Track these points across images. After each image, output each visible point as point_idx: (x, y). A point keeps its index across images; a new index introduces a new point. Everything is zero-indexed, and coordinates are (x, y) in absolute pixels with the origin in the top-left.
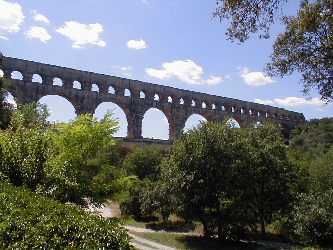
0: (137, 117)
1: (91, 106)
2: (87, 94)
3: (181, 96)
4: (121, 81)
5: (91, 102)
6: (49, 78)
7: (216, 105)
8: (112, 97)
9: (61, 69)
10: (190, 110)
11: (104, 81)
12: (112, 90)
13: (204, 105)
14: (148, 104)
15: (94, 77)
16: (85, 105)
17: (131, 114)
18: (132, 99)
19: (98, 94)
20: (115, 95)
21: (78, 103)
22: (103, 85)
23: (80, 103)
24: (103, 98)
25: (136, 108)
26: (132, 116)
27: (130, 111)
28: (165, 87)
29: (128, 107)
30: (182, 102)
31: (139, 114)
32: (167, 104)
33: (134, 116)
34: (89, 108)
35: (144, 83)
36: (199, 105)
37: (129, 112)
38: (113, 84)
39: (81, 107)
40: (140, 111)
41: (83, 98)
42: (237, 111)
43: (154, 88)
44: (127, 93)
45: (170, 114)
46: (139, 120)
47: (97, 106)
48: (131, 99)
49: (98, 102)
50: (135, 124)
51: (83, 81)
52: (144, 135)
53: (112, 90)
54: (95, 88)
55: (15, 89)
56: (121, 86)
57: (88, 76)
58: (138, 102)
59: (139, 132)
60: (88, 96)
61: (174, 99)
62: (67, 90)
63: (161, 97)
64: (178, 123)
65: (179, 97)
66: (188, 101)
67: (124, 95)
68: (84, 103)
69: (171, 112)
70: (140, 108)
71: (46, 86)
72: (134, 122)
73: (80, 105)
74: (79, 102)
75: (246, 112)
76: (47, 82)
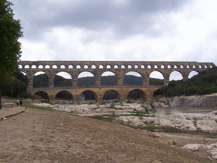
4: (89, 62)
6: (59, 66)
13: (136, 67)
31: (99, 76)
36: (133, 67)
41: (73, 72)
42: (159, 67)
49: (80, 73)
54: (78, 67)
55: (47, 72)
56: (90, 65)
65: (120, 65)
66: (126, 66)
70: (99, 73)
74: (71, 74)
76: (59, 68)
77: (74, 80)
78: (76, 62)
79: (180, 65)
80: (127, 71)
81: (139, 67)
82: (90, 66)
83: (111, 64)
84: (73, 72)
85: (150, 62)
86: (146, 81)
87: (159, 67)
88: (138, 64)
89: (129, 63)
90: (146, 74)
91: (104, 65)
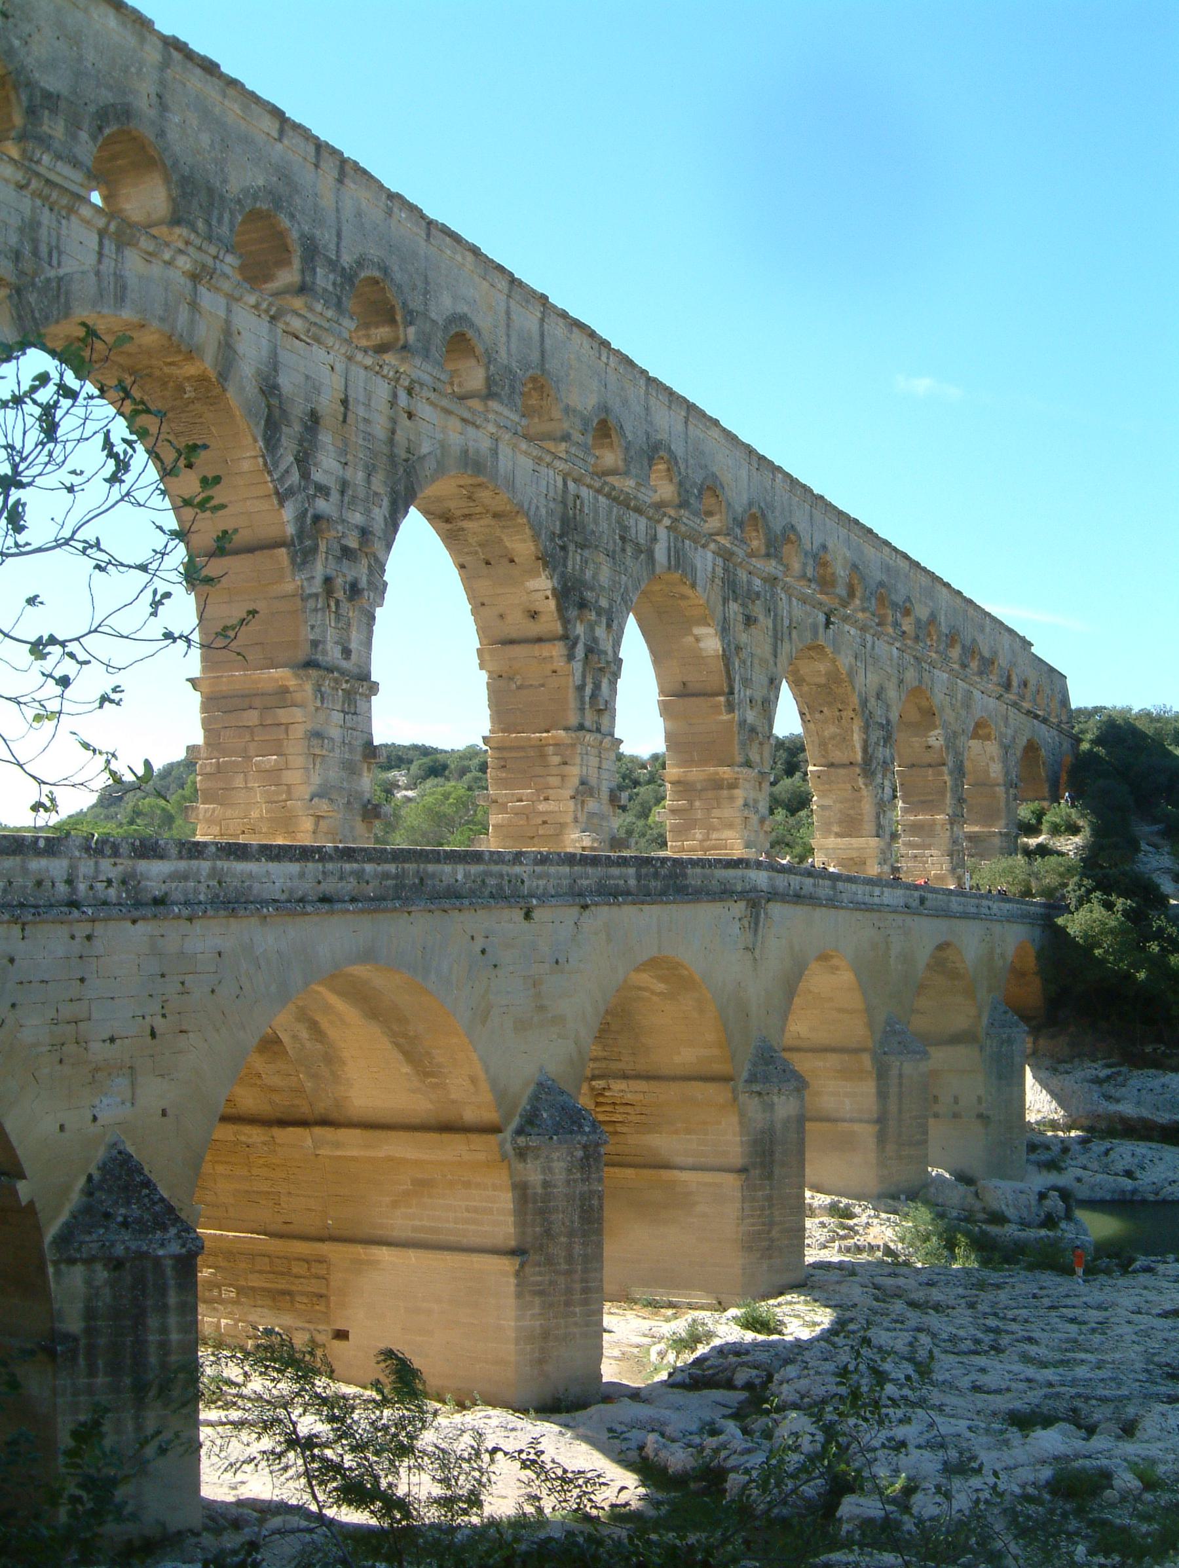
1: (357, 518)
5: (360, 475)
10: (786, 623)
17: (566, 622)
18: (571, 485)
21: (283, 467)
23: (295, 477)
24: (425, 449)
28: (691, 409)
33: (580, 651)
34: (353, 543)
39: (301, 517)
41: (314, 418)
68: (317, 476)
69: (724, 631)
71: (46, 217)
77: (333, 654)
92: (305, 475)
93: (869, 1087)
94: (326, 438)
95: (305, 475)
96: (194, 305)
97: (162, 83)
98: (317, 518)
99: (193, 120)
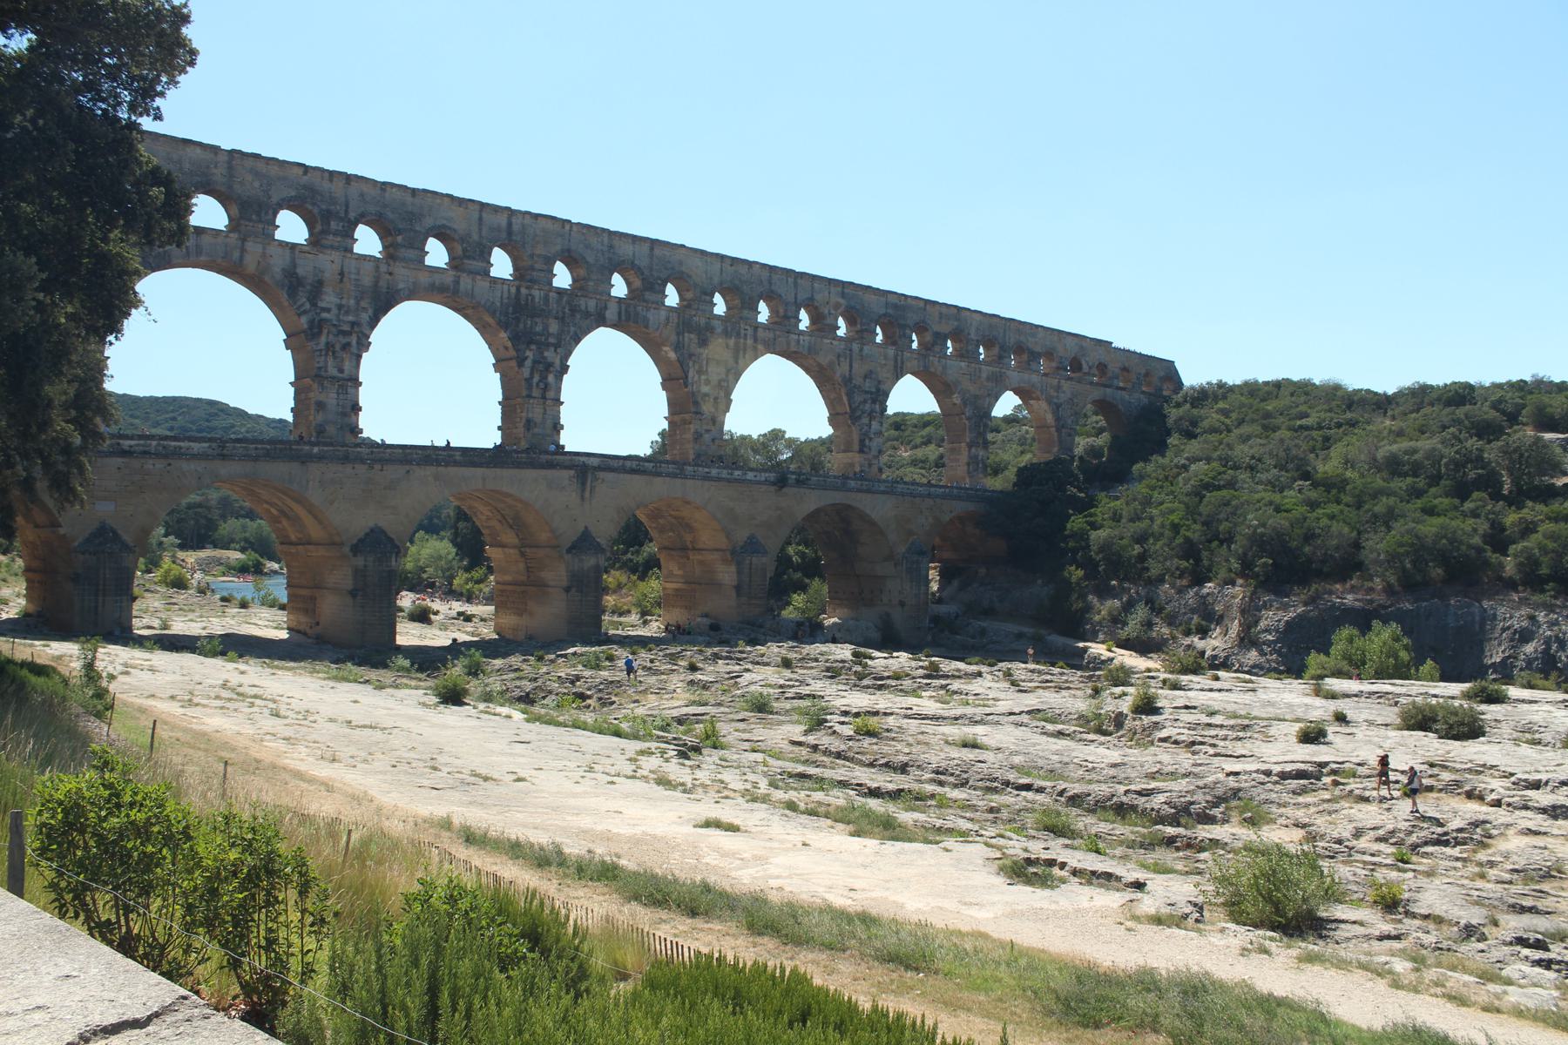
0: (541, 367)
1: (351, 318)
2: (336, 267)
3: (716, 280)
5: (352, 302)
7: (850, 322)
8: (437, 279)
9: (223, 158)
11: (405, 213)
12: (436, 254)
13: (805, 321)
14: (587, 314)
15: (362, 195)
16: (325, 315)
18: (524, 291)
19: (383, 268)
20: (452, 273)
22: (400, 232)
23: (308, 306)
24: (401, 286)
25: (539, 328)
26: (521, 363)
27: (515, 338)
28: (654, 243)
29: (505, 326)
30: (720, 307)
31: (549, 354)
32: (663, 313)
33: (528, 363)
34: (346, 328)
35: (567, 227)
36: (783, 320)
37: (509, 344)
38: (444, 226)
39: (311, 322)
40: (551, 340)
43: (611, 247)
44: (501, 265)
45: (672, 355)
46: (551, 378)
47: (378, 320)
48: (518, 289)
49: (384, 303)
50: (536, 393)
51: (316, 211)
52: (574, 439)
53: (436, 254)
54: (367, 242)
57: (338, 188)
58: (546, 298)
59: (549, 423)
60: (342, 274)
61: (689, 295)
62: (249, 245)
63: (638, 283)
64: (705, 389)
66: (743, 303)
67: (487, 273)
69: (678, 347)
70: (554, 327)
72: (530, 387)
73: (305, 312)
74: (302, 299)
75: (966, 354)
77: (332, 371)
78: (354, 189)
79: (1038, 349)
80: (755, 349)
81: (822, 324)
82: (468, 255)
83: (643, 262)
84: (319, 285)
85: (891, 298)
86: (862, 442)
87: (933, 344)
88: (818, 297)
89: (766, 274)
90: (868, 385)
91: (591, 260)
92: (314, 305)
93: (733, 569)
94: (328, 289)
95: (314, 305)
96: (243, 250)
97: (230, 168)
98: (322, 321)
99: (249, 178)
